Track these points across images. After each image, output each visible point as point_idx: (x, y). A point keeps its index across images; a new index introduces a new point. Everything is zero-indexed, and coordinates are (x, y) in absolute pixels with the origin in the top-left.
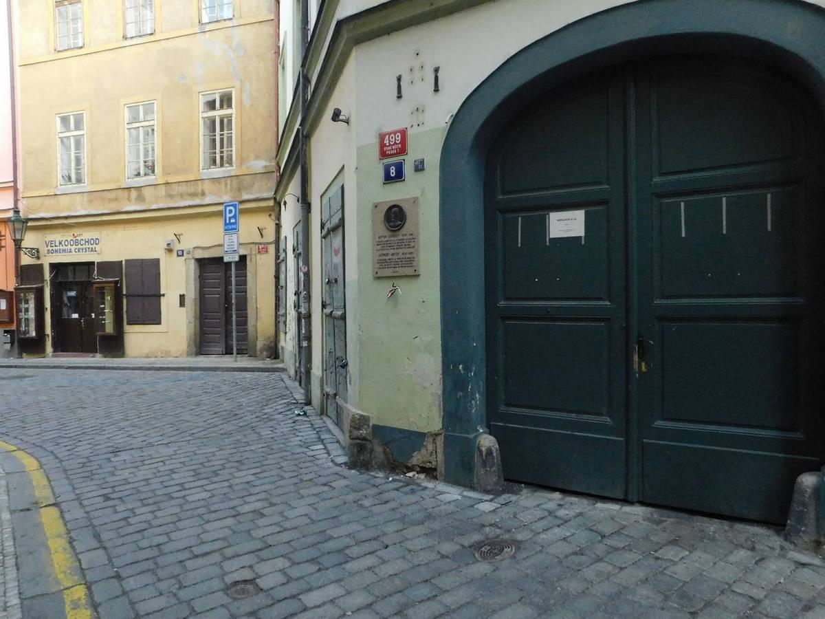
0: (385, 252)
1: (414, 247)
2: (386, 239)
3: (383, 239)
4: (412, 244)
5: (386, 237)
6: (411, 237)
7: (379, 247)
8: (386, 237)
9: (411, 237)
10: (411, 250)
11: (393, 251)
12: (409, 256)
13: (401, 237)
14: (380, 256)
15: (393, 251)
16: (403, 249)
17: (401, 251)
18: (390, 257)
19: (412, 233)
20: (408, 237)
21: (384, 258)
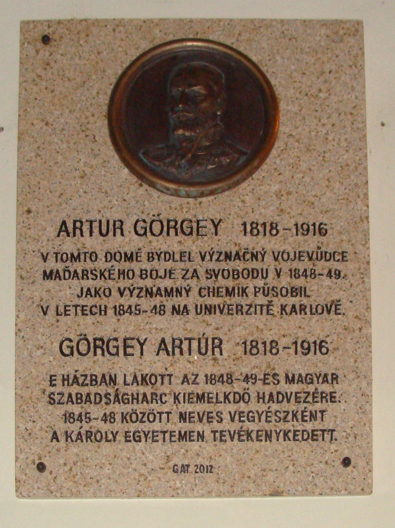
0: (108, 327)
1: (333, 308)
2: (116, 243)
3: (92, 243)
4: (321, 290)
5: (118, 227)
6: (311, 243)
7: (67, 291)
8: (118, 227)
9: (311, 243)
10: (315, 328)
11: (172, 327)
12: (299, 365)
13: (231, 239)
14: (68, 349)
15: (172, 327)
16: (255, 320)
17: (235, 329)
18: (152, 363)
19: (312, 217)
20: (289, 243)
21: (98, 364)
